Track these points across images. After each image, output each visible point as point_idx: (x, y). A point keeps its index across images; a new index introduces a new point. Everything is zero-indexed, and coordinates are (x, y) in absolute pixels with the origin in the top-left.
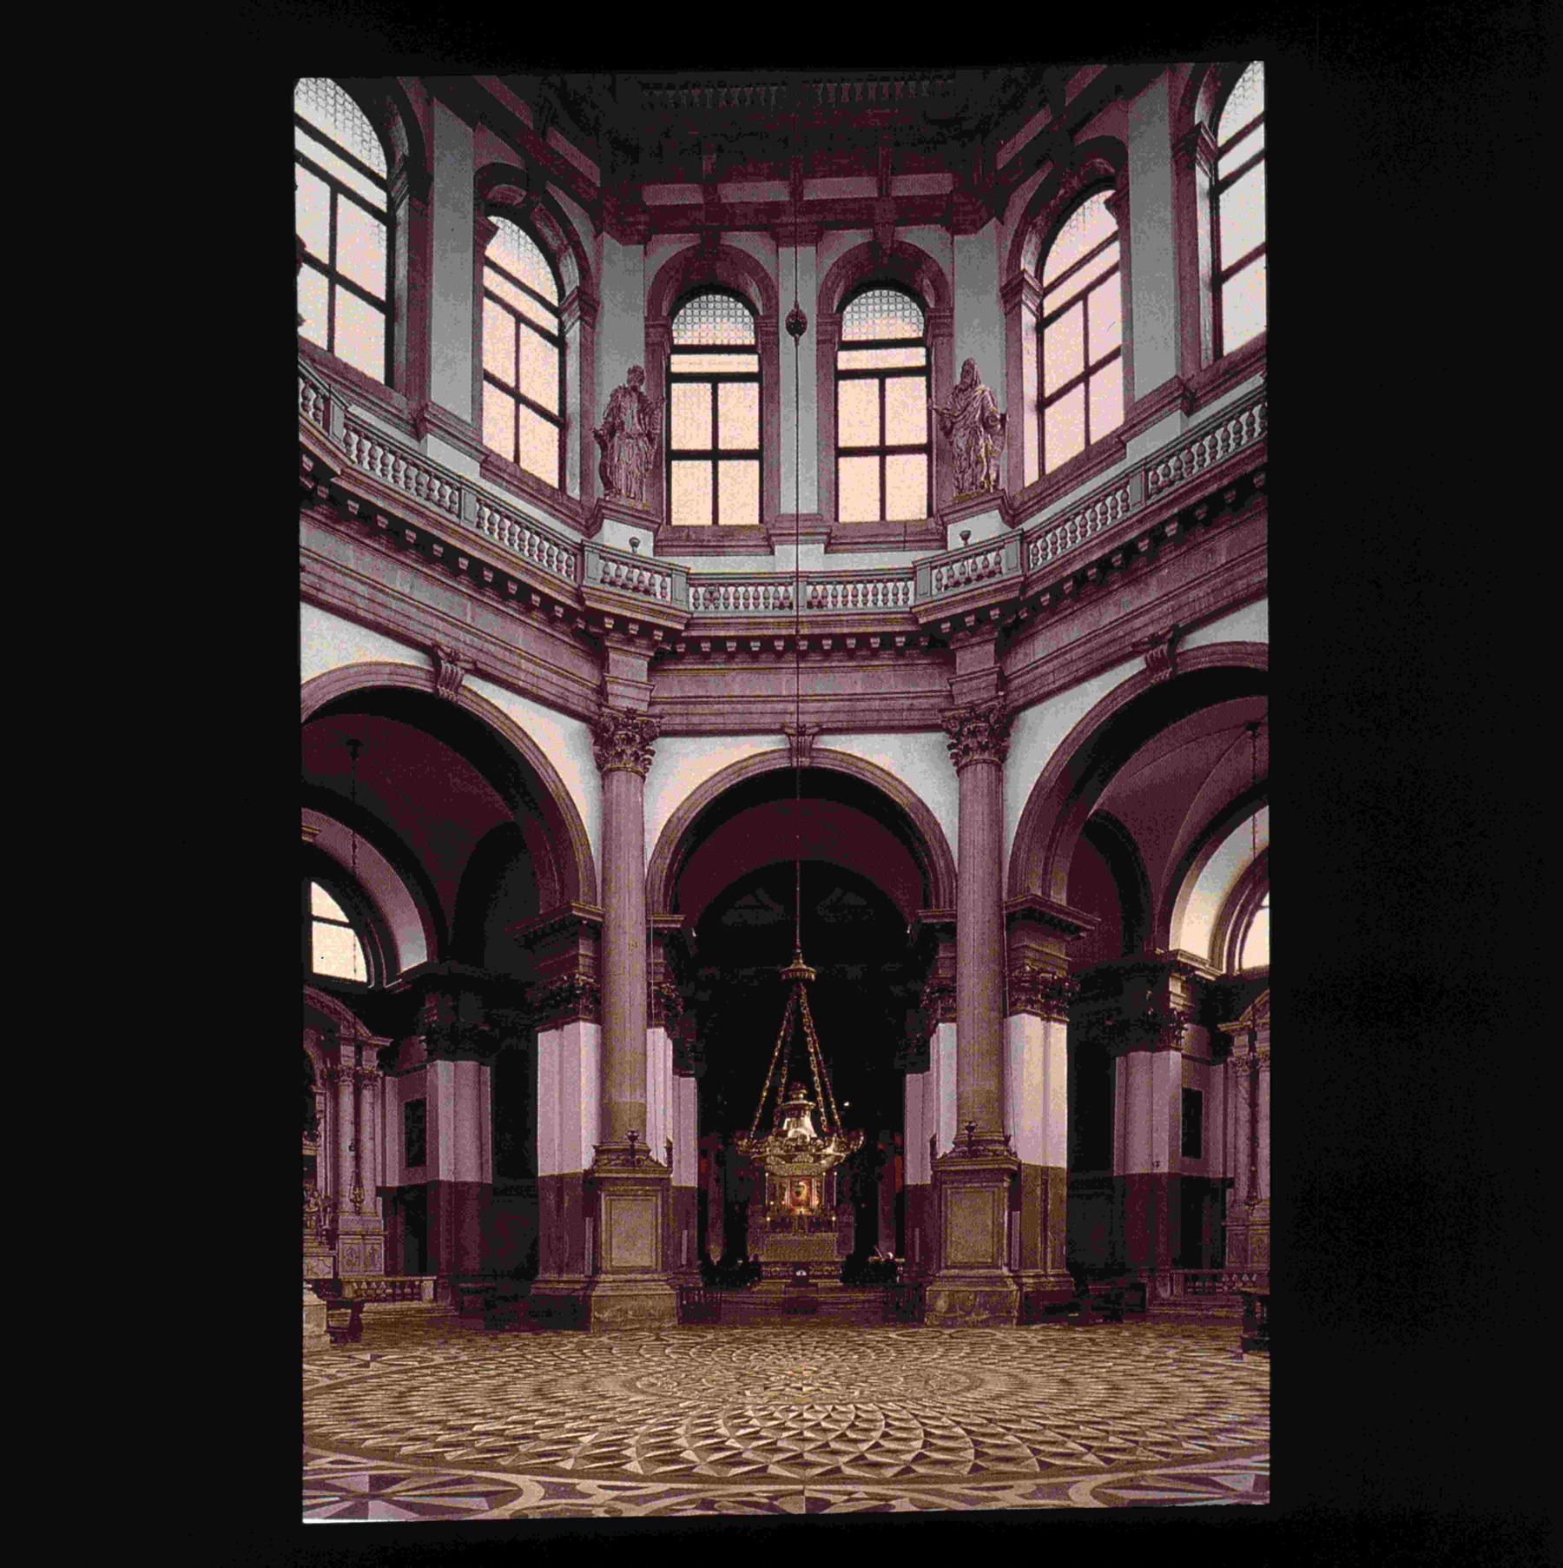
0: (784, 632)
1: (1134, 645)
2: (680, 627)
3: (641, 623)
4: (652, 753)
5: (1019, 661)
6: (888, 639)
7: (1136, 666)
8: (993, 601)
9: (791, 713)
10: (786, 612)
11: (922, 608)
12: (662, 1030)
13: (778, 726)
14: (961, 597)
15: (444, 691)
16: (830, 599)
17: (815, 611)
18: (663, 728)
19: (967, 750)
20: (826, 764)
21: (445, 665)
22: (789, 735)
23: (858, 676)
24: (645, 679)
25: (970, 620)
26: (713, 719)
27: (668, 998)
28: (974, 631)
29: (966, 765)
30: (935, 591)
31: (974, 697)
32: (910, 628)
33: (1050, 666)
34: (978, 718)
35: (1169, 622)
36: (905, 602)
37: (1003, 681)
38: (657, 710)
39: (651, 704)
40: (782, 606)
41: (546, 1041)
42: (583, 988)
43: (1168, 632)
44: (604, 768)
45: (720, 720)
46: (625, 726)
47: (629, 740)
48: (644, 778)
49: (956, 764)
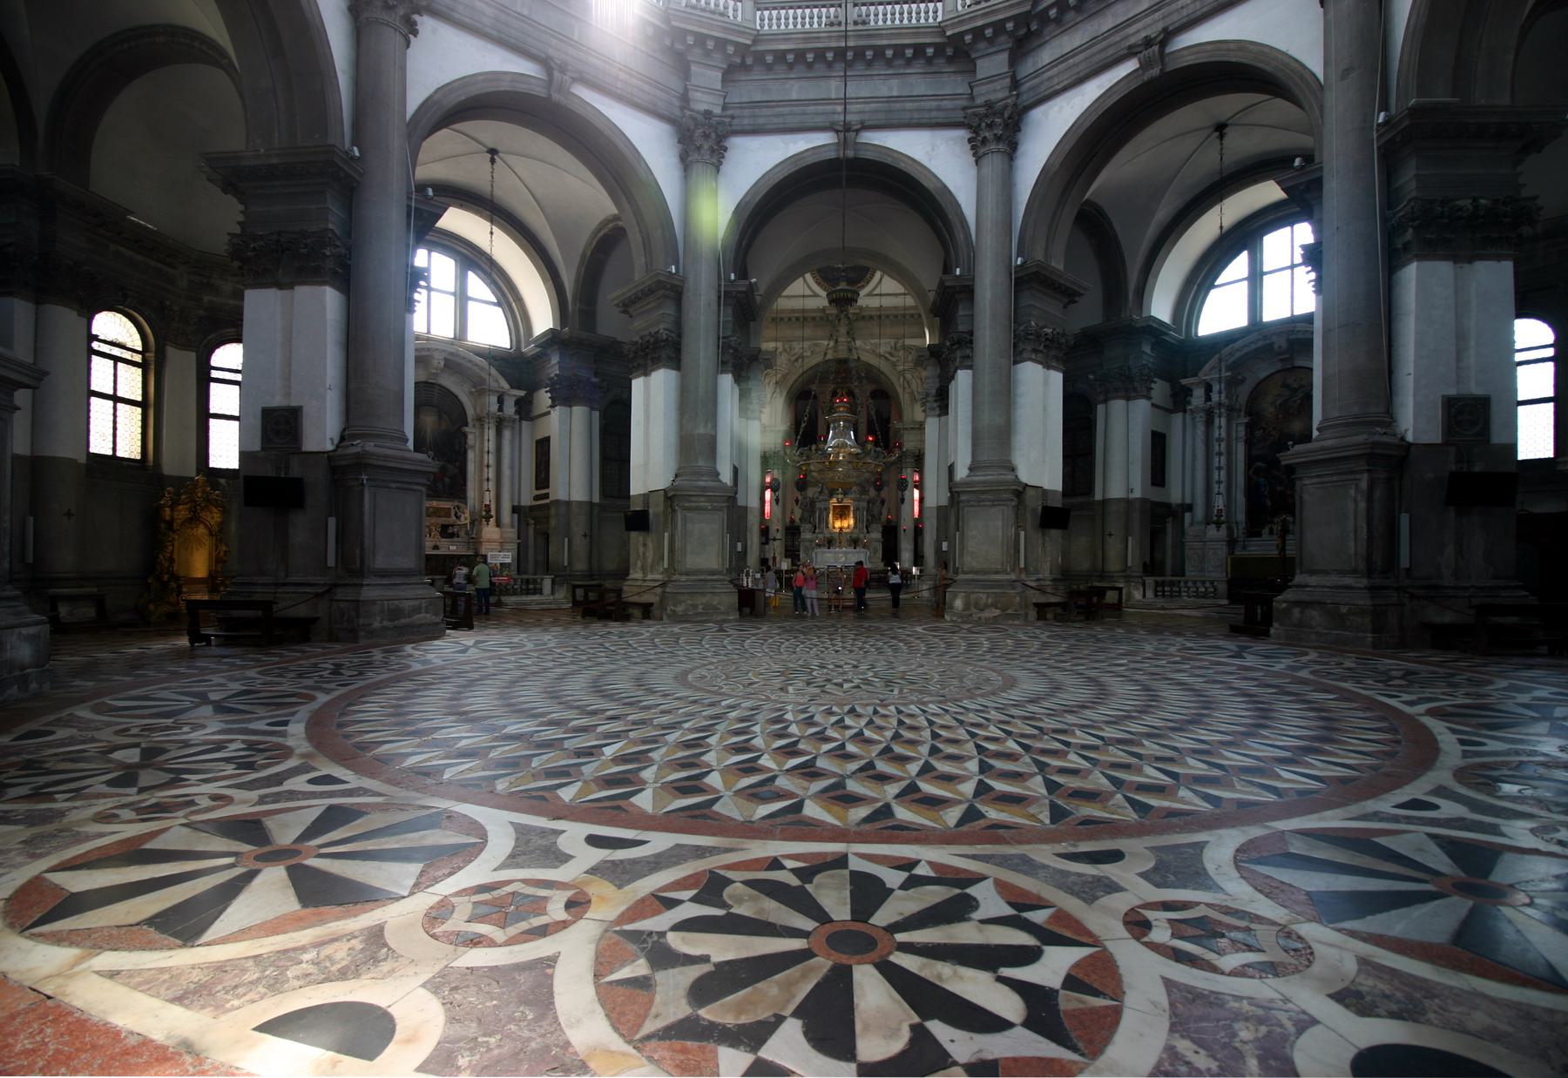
0: (834, 45)
1: (1130, 47)
2: (749, 42)
3: (717, 39)
4: (726, 149)
5: (1027, 68)
6: (919, 50)
7: (1130, 66)
8: (1008, 15)
9: (839, 113)
10: (836, 28)
11: (949, 23)
12: (730, 375)
13: (828, 124)
14: (982, 12)
15: (556, 96)
16: (872, 17)
17: (860, 27)
18: (734, 128)
19: (984, 141)
20: (869, 155)
21: (556, 74)
22: (837, 132)
23: (894, 82)
24: (719, 88)
25: (989, 32)
26: (775, 120)
27: (736, 350)
28: (991, 41)
29: (985, 154)
30: (960, 8)
31: (993, 97)
32: (938, 40)
33: (1055, 71)
34: (994, 114)
35: (1160, 26)
36: (935, 19)
37: (1015, 84)
38: (730, 112)
39: (724, 108)
40: (832, 24)
41: (637, 384)
42: (667, 339)
43: (1158, 36)
44: (685, 163)
45: (781, 120)
46: (702, 126)
47: (706, 136)
48: (718, 171)
49: (974, 155)
